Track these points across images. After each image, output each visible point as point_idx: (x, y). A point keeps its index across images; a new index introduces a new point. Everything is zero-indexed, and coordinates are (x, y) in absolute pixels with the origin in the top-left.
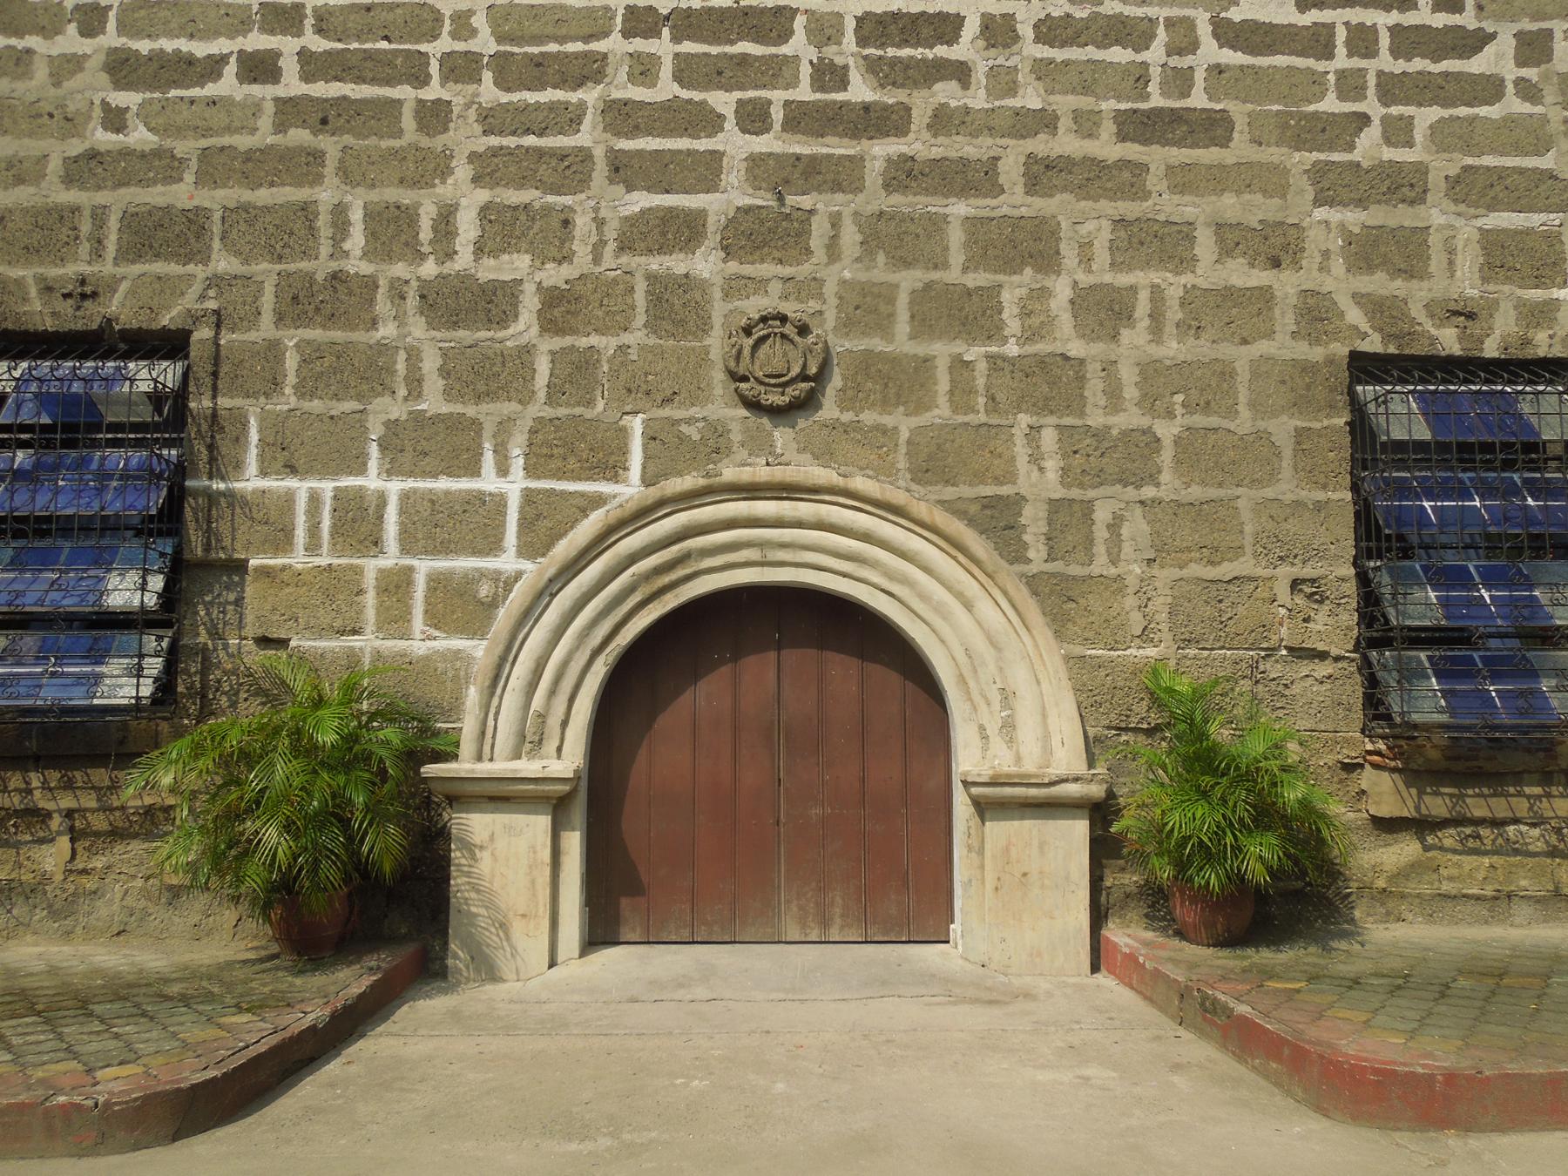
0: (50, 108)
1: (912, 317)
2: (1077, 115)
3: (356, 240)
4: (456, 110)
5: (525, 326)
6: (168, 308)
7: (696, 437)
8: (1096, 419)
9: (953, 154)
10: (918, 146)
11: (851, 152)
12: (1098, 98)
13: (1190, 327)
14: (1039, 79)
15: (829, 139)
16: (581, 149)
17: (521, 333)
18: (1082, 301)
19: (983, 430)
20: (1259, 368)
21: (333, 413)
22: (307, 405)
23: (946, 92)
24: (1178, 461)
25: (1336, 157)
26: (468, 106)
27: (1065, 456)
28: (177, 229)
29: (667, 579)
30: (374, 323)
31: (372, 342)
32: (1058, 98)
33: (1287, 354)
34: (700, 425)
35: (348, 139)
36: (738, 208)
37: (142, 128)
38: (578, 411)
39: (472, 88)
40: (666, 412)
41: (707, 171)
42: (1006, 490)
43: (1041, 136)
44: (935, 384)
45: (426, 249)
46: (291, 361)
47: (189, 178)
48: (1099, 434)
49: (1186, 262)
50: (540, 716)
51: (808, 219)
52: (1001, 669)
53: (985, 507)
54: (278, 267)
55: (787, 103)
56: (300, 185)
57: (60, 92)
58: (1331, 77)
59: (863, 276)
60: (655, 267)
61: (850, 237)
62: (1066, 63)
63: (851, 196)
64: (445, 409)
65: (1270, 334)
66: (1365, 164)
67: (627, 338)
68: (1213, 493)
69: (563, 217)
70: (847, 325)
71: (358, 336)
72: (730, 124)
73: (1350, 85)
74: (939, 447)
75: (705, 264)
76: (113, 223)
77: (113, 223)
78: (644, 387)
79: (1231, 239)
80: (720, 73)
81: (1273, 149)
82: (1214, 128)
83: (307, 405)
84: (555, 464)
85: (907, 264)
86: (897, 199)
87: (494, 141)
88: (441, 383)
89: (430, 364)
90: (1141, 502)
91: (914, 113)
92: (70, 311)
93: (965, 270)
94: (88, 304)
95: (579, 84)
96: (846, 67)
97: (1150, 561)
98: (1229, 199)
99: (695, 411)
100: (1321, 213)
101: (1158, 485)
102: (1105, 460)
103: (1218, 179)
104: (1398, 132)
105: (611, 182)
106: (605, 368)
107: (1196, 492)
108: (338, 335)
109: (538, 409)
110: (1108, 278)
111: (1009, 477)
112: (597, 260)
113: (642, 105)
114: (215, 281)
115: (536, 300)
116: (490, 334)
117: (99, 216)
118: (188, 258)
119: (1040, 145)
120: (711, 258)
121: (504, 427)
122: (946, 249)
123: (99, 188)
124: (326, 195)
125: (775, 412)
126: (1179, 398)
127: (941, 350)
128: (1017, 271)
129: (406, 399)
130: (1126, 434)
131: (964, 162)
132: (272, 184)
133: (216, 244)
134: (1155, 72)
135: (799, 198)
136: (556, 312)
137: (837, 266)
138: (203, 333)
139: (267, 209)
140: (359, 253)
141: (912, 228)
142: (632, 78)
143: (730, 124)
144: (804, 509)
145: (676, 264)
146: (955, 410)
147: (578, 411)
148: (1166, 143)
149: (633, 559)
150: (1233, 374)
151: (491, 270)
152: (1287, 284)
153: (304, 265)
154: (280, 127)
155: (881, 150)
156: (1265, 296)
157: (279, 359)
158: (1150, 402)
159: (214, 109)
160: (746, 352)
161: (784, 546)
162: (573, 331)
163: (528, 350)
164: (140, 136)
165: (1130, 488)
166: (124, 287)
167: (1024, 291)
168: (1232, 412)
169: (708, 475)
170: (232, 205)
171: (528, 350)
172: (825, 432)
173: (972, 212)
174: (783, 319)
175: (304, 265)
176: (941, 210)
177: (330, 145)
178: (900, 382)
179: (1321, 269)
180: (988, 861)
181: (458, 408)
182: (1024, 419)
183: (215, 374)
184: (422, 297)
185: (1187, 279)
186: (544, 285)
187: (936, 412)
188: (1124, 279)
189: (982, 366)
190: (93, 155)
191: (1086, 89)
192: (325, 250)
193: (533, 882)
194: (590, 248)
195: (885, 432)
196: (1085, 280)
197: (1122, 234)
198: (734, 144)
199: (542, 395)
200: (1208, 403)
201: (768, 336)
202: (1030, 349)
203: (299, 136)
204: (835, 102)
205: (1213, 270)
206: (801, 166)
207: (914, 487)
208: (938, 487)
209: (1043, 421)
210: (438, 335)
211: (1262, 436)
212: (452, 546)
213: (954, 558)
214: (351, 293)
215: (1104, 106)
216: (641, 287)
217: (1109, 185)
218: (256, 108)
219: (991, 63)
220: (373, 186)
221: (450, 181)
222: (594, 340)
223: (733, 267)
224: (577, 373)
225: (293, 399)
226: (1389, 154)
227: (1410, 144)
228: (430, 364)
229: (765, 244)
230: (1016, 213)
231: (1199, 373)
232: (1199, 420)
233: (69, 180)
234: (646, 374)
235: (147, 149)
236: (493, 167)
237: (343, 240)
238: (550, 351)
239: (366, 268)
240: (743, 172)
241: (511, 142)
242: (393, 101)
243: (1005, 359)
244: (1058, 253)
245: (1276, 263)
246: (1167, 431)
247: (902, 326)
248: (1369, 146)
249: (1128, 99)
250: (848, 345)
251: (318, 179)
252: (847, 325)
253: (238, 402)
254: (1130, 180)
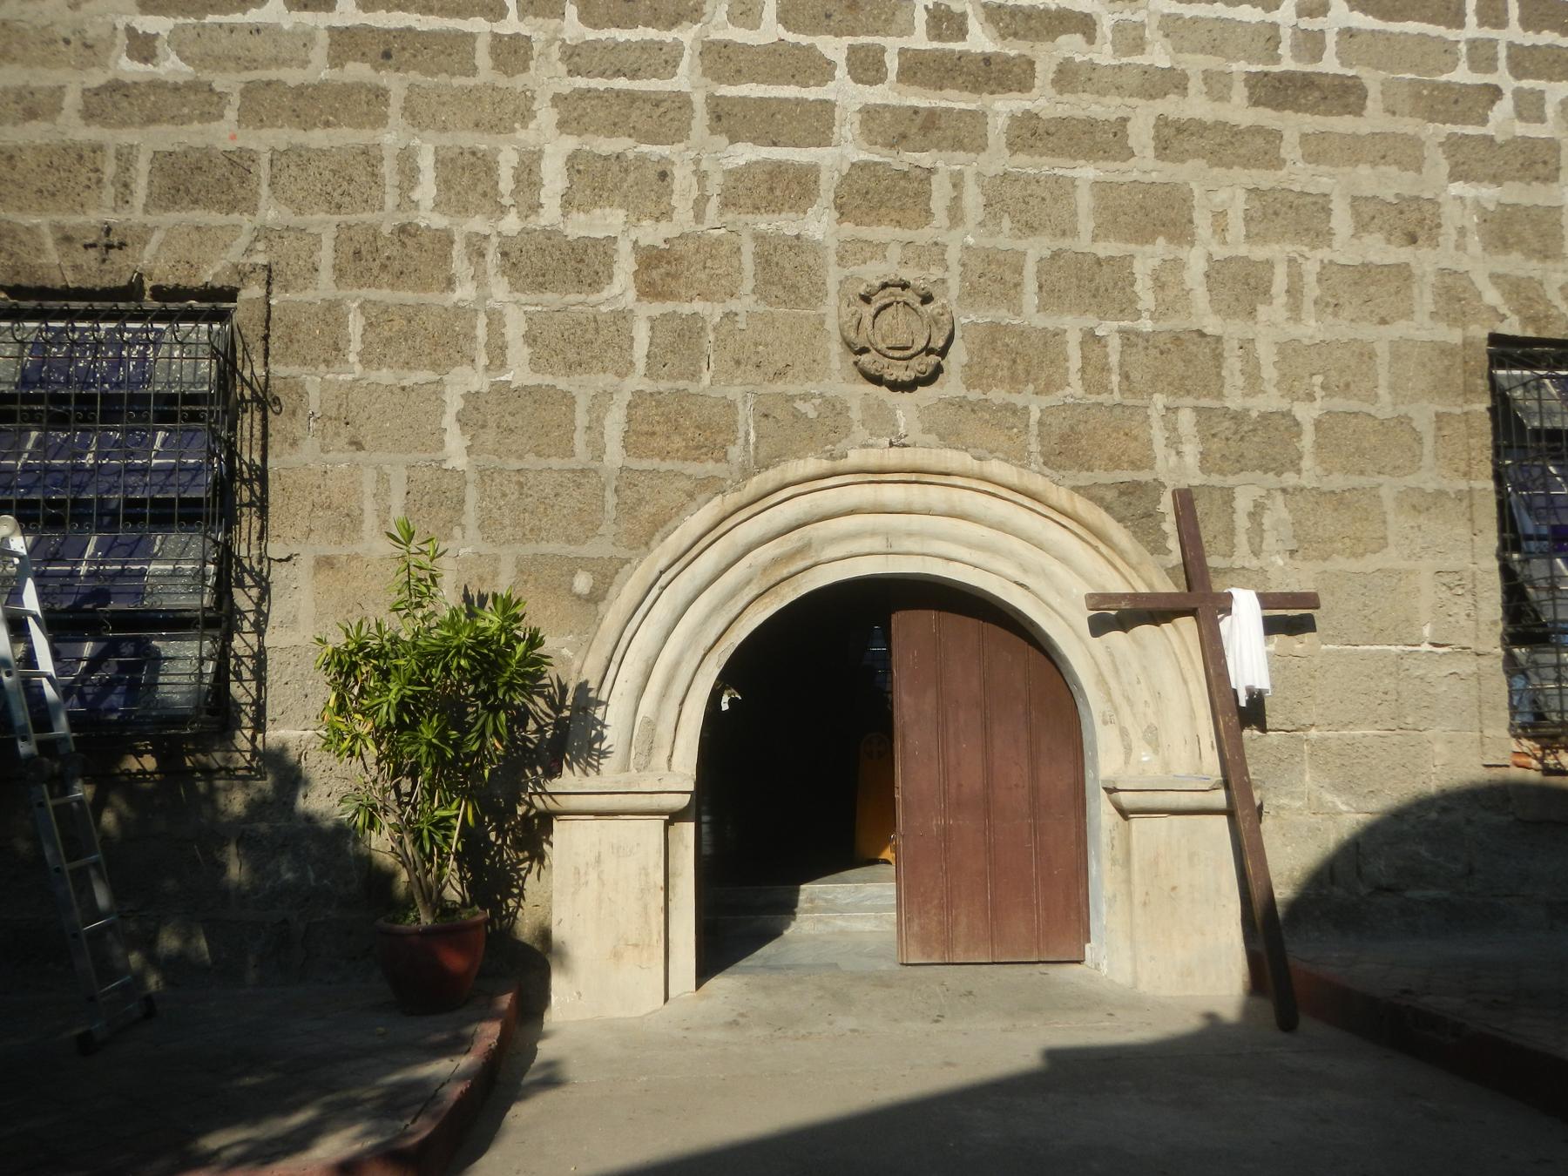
0: (67, 33)
1: (1040, 287)
2: (1208, 76)
3: (427, 189)
4: (537, 47)
5: (621, 286)
6: (210, 263)
7: (812, 414)
8: (1234, 402)
9: (1079, 114)
10: (1042, 102)
11: (972, 107)
12: (1229, 59)
13: (1327, 305)
14: (1167, 36)
15: (948, 92)
16: (679, 94)
17: (616, 297)
18: (1217, 273)
19: (1117, 411)
20: (1398, 351)
21: (405, 383)
22: (374, 376)
23: (1070, 46)
24: (1319, 446)
25: (1470, 130)
26: (549, 43)
27: (1203, 440)
28: (218, 173)
29: (785, 572)
30: (450, 283)
31: (448, 304)
32: (1187, 56)
33: (1424, 335)
34: (818, 401)
35: (414, 76)
36: (853, 164)
37: (174, 57)
38: (681, 384)
39: (554, 23)
40: (779, 386)
41: (815, 123)
42: (1144, 476)
43: (1172, 97)
44: (1066, 360)
45: (507, 201)
46: (355, 325)
47: (231, 114)
48: (1238, 417)
49: (1323, 236)
50: (649, 722)
51: (928, 179)
52: (1145, 668)
53: (1122, 493)
54: (337, 218)
55: (902, 52)
56: (361, 126)
57: (78, 15)
58: (1463, 48)
59: (988, 243)
60: (763, 226)
61: (973, 199)
62: (1195, 20)
63: (973, 155)
64: (533, 380)
65: (1408, 314)
66: (1499, 139)
67: (733, 305)
68: (1356, 481)
69: (659, 168)
70: (971, 294)
71: (432, 297)
72: (841, 72)
73: (1482, 55)
74: (1072, 428)
75: (819, 224)
76: (143, 165)
77: (143, 165)
78: (754, 359)
79: (1367, 214)
80: (828, 16)
81: (1407, 119)
82: (1346, 95)
83: (374, 376)
84: (658, 442)
85: (1031, 228)
86: (1022, 158)
87: (581, 82)
88: (527, 351)
89: (514, 329)
90: (1284, 490)
91: (1038, 67)
92: (95, 265)
93: (1095, 239)
94: (114, 253)
95: (673, 23)
96: (964, 15)
97: (1292, 552)
98: (1364, 170)
99: (811, 387)
100: (1457, 188)
101: (1299, 472)
102: (1245, 445)
103: (1354, 150)
104: (1530, 107)
105: (713, 131)
106: (711, 337)
107: (1338, 481)
108: (409, 296)
109: (637, 381)
110: (1243, 250)
111: (1147, 461)
112: (699, 217)
113: (745, 48)
114: (264, 234)
115: (632, 259)
116: (582, 297)
117: (125, 158)
118: (232, 207)
119: (1171, 107)
120: (825, 219)
121: (602, 399)
122: (1075, 214)
123: (123, 124)
124: (390, 138)
125: (895, 386)
126: (1318, 379)
127: (1072, 325)
128: (1150, 239)
129: (487, 368)
130: (1265, 416)
131: (1091, 124)
132: (327, 124)
133: (264, 190)
134: (1286, 34)
135: (917, 155)
136: (655, 274)
137: (960, 231)
138: (252, 291)
139: (323, 152)
140: (430, 204)
141: (1039, 191)
142: (732, 18)
143: (841, 72)
144: (934, 495)
145: (784, 224)
146: (1088, 390)
147: (681, 384)
148: (1298, 109)
150: (1372, 355)
151: (579, 226)
152: (1426, 261)
153: (367, 217)
154: (336, 60)
155: (1003, 107)
156: (1403, 273)
157: (341, 322)
158: (1287, 386)
159: (258, 38)
160: (867, 321)
161: (910, 534)
162: (672, 295)
163: (623, 317)
164: (170, 67)
165: (1271, 474)
166: (157, 237)
167: (1156, 262)
169: (832, 458)
170: (282, 148)
171: (624, 316)
172: (952, 410)
173: (1101, 176)
174: (905, 286)
175: (367, 217)
176: (1069, 173)
177: (394, 82)
178: (1027, 359)
179: (1457, 247)
180: (1136, 878)
181: (548, 380)
182: (1160, 400)
183: (266, 338)
184: (505, 254)
185: (1324, 254)
186: (642, 243)
187: (1068, 390)
188: (1259, 253)
189: (1115, 343)
190: (117, 87)
191: (1214, 49)
192: (391, 200)
193: (645, 907)
194: (691, 203)
195: (1014, 412)
196: (1220, 252)
197: (1257, 204)
198: (846, 93)
199: (641, 365)
200: (1347, 385)
201: (890, 304)
202: (1165, 325)
203: (358, 71)
204: (953, 51)
205: (1348, 245)
206: (919, 120)
207: (1047, 471)
208: (1074, 471)
209: (1179, 402)
210: (523, 298)
211: (1404, 421)
212: (544, 534)
213: (1096, 549)
214: (420, 247)
215: (1234, 67)
216: (748, 248)
217: (1242, 151)
218: (308, 39)
219: (1117, 16)
220: (445, 129)
221: (532, 125)
222: (698, 306)
223: (848, 228)
224: (680, 342)
225: (358, 368)
226: (1521, 129)
227: (1541, 119)
228: (514, 329)
229: (882, 203)
230: (1147, 179)
231: (1338, 353)
232: (1339, 404)
233: (88, 115)
234: (756, 344)
235: (180, 80)
236: (579, 111)
237: (412, 188)
238: (649, 318)
239: (439, 221)
240: (857, 125)
241: (599, 84)
242: (465, 34)
243: (1138, 334)
244: (1191, 221)
245: (1413, 239)
246: (1307, 413)
247: (1030, 296)
248: (1501, 120)
249: (1259, 61)
250: (973, 317)
251: (381, 121)
252: (971, 294)
253: (294, 370)
254: (1261, 148)
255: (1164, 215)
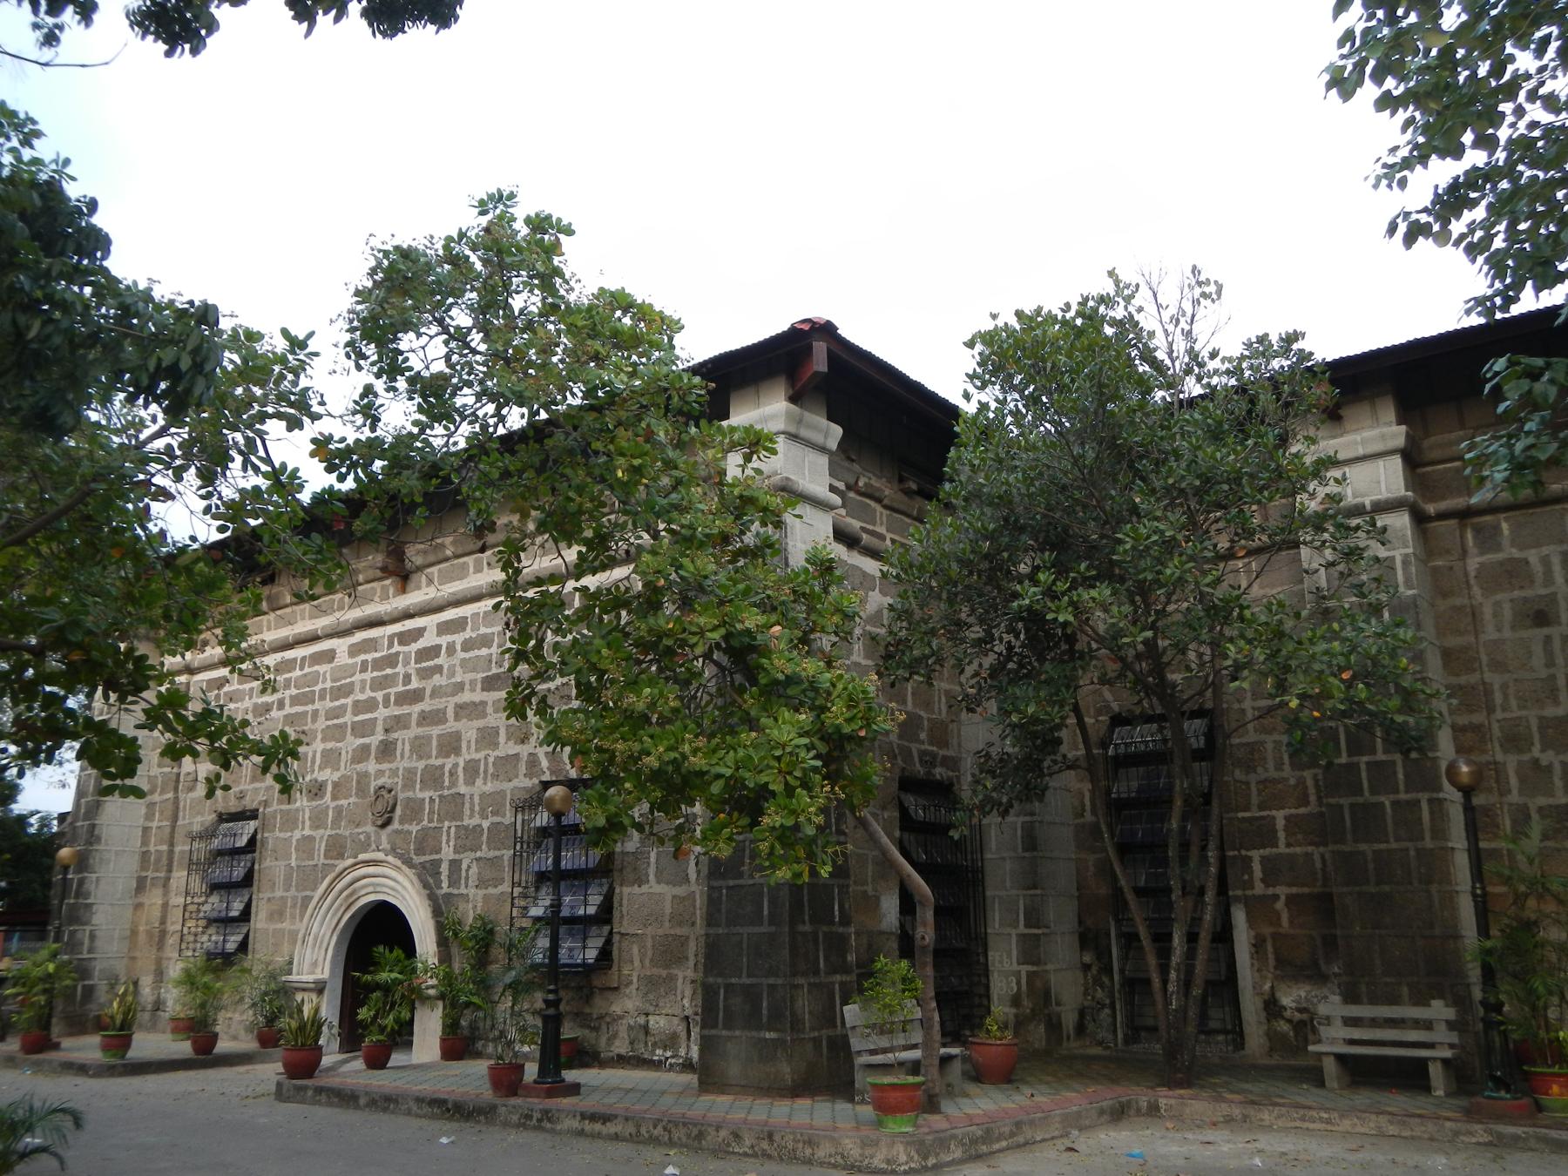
48: (466, 828)
49: (495, 745)
149: (341, 892)
168: (504, 816)
185: (497, 753)
255: (451, 745)
